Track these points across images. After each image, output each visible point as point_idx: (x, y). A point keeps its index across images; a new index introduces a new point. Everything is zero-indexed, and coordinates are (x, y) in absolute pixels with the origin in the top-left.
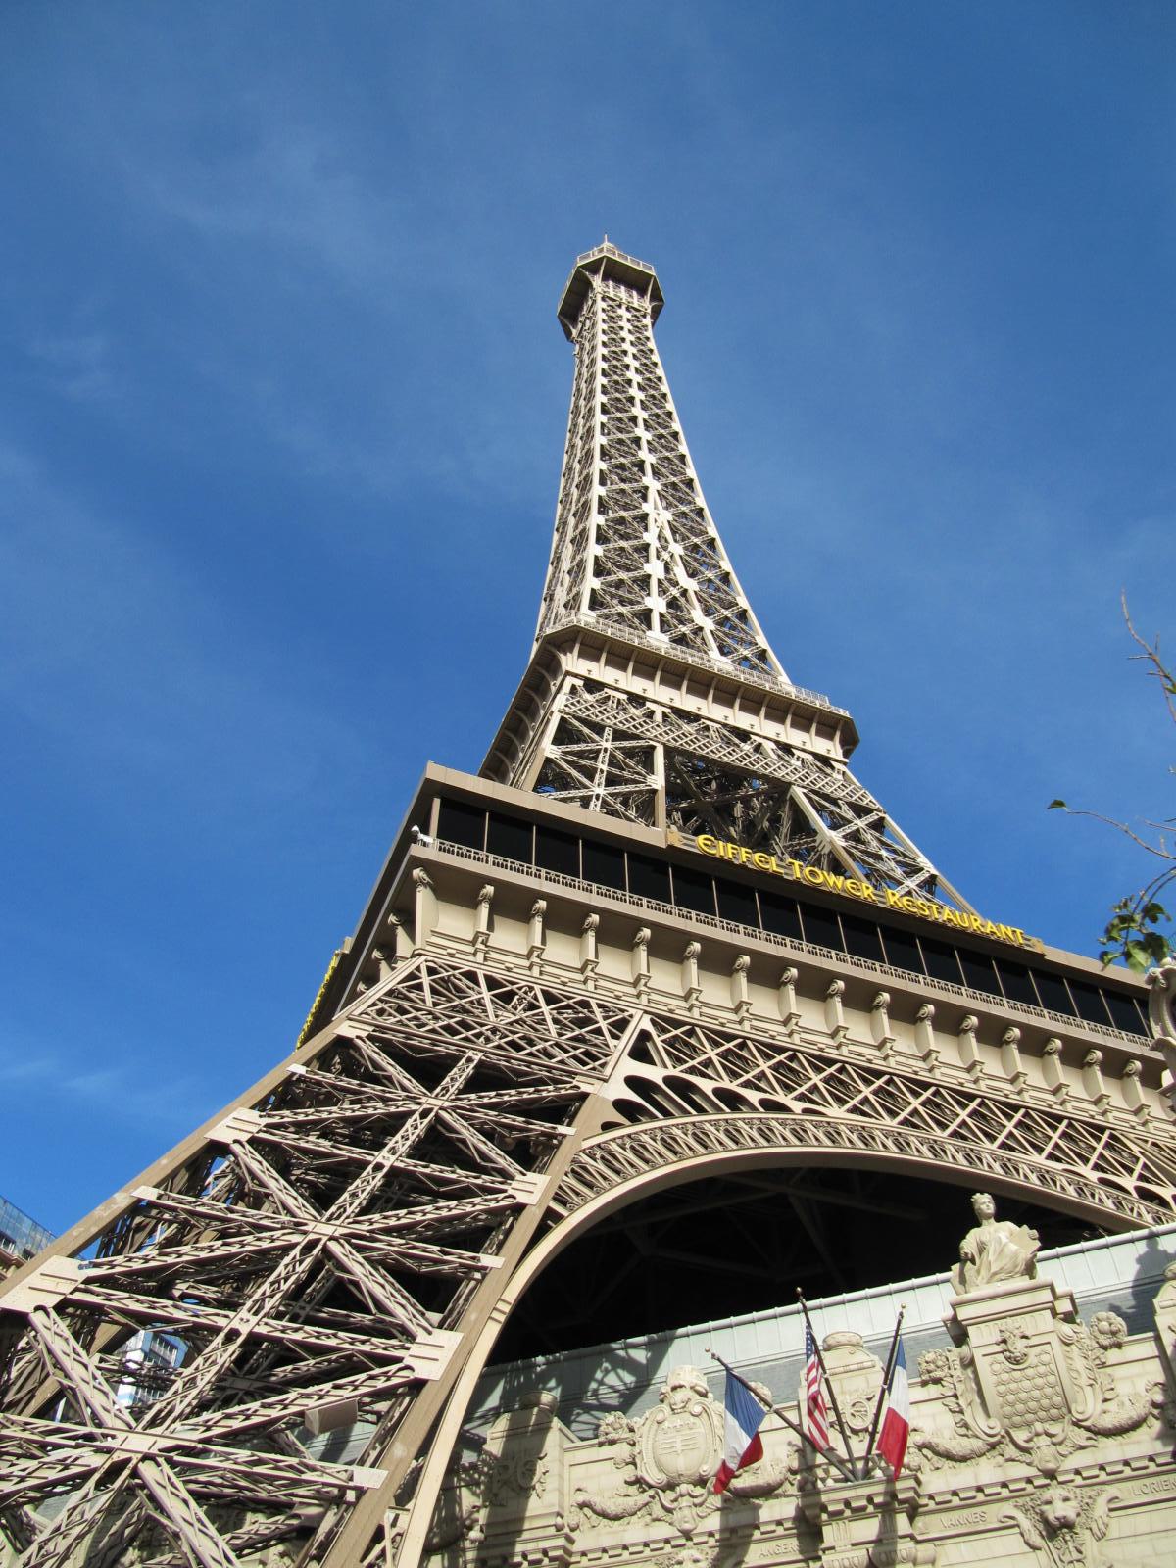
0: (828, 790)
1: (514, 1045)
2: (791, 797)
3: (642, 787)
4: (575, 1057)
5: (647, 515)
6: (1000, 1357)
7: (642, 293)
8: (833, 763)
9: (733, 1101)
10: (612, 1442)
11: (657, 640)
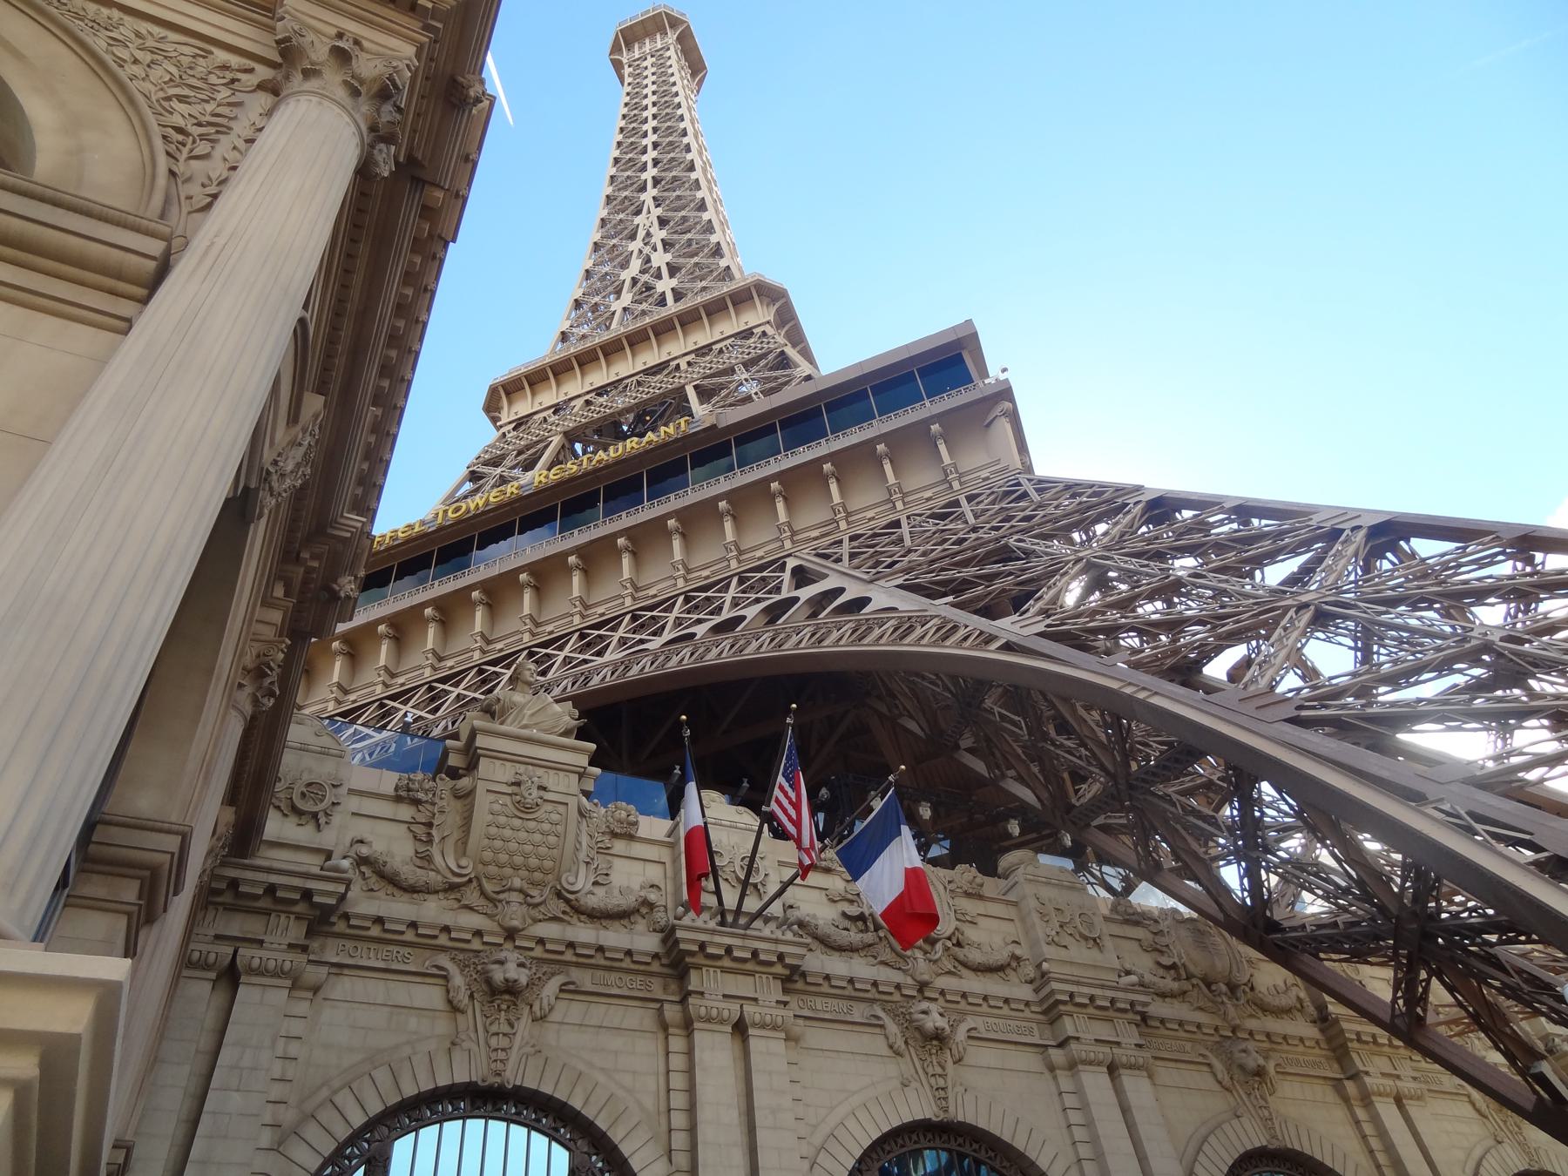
6: (507, 800)
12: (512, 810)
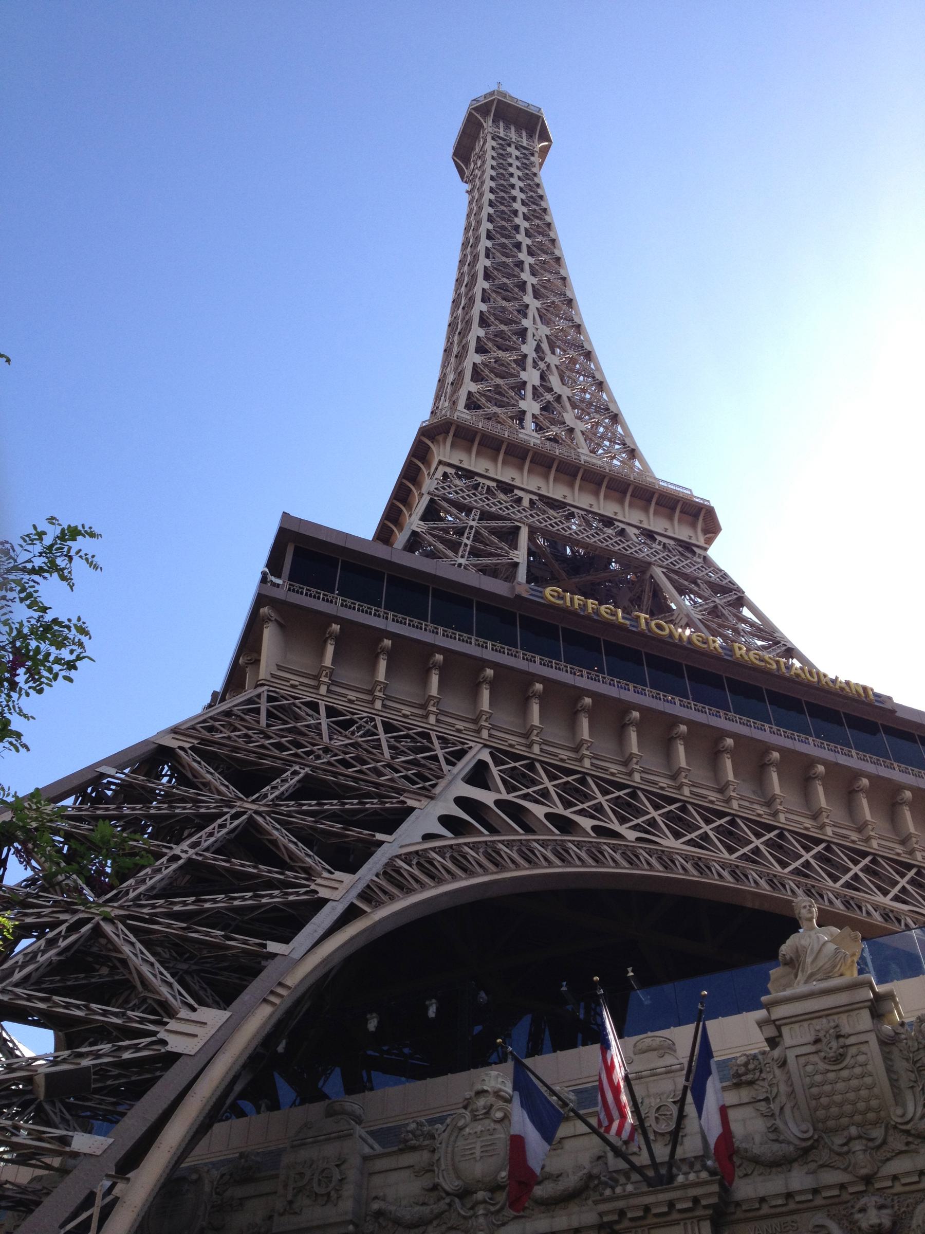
0: (688, 571)
1: (346, 764)
2: (652, 577)
3: (504, 560)
4: (406, 777)
5: (526, 329)
6: (815, 1058)
7: (530, 136)
8: (695, 549)
9: (565, 825)
10: (414, 1149)
11: (529, 434)
12: (822, 1066)
